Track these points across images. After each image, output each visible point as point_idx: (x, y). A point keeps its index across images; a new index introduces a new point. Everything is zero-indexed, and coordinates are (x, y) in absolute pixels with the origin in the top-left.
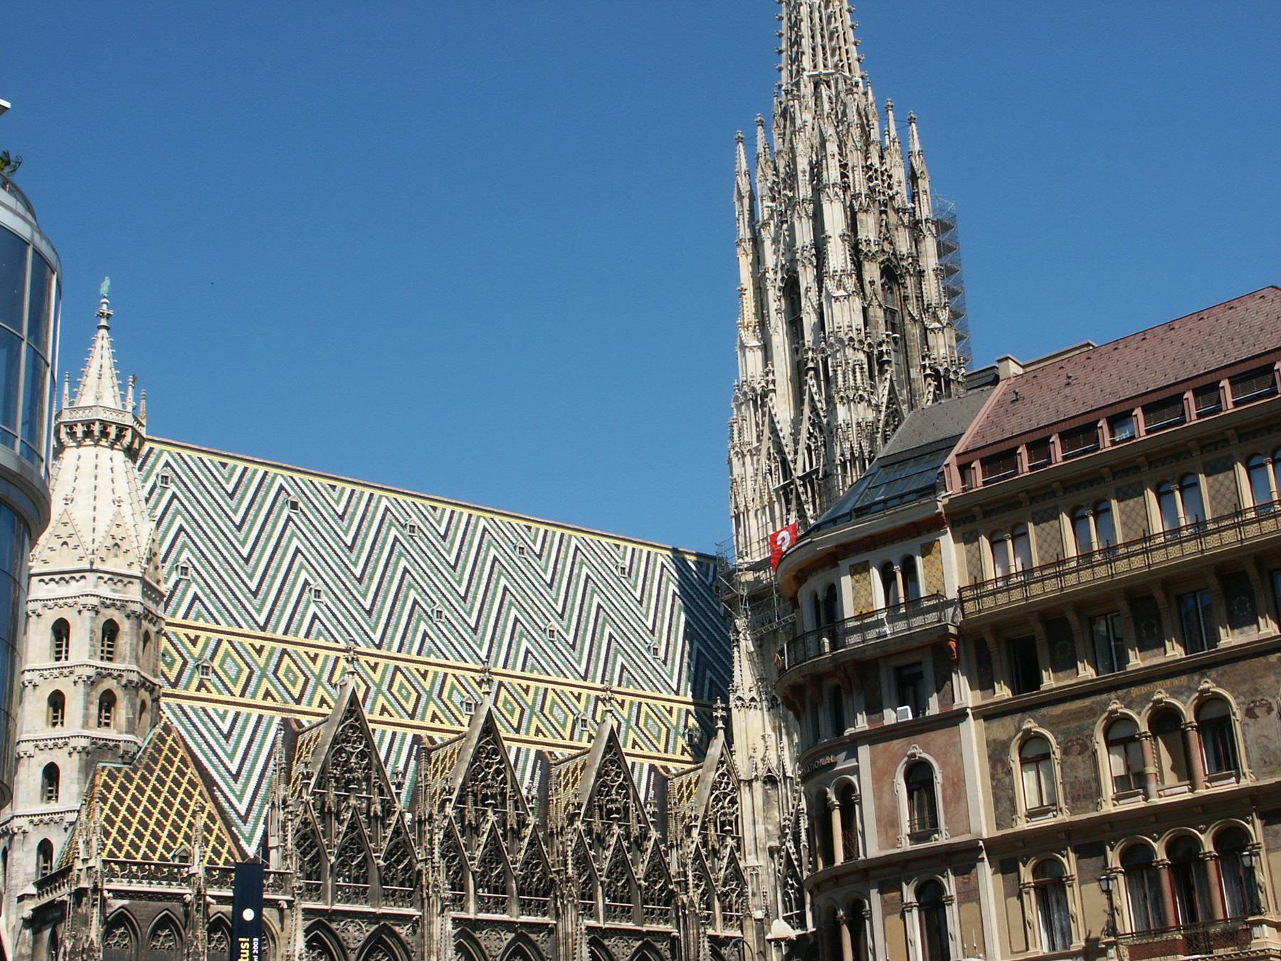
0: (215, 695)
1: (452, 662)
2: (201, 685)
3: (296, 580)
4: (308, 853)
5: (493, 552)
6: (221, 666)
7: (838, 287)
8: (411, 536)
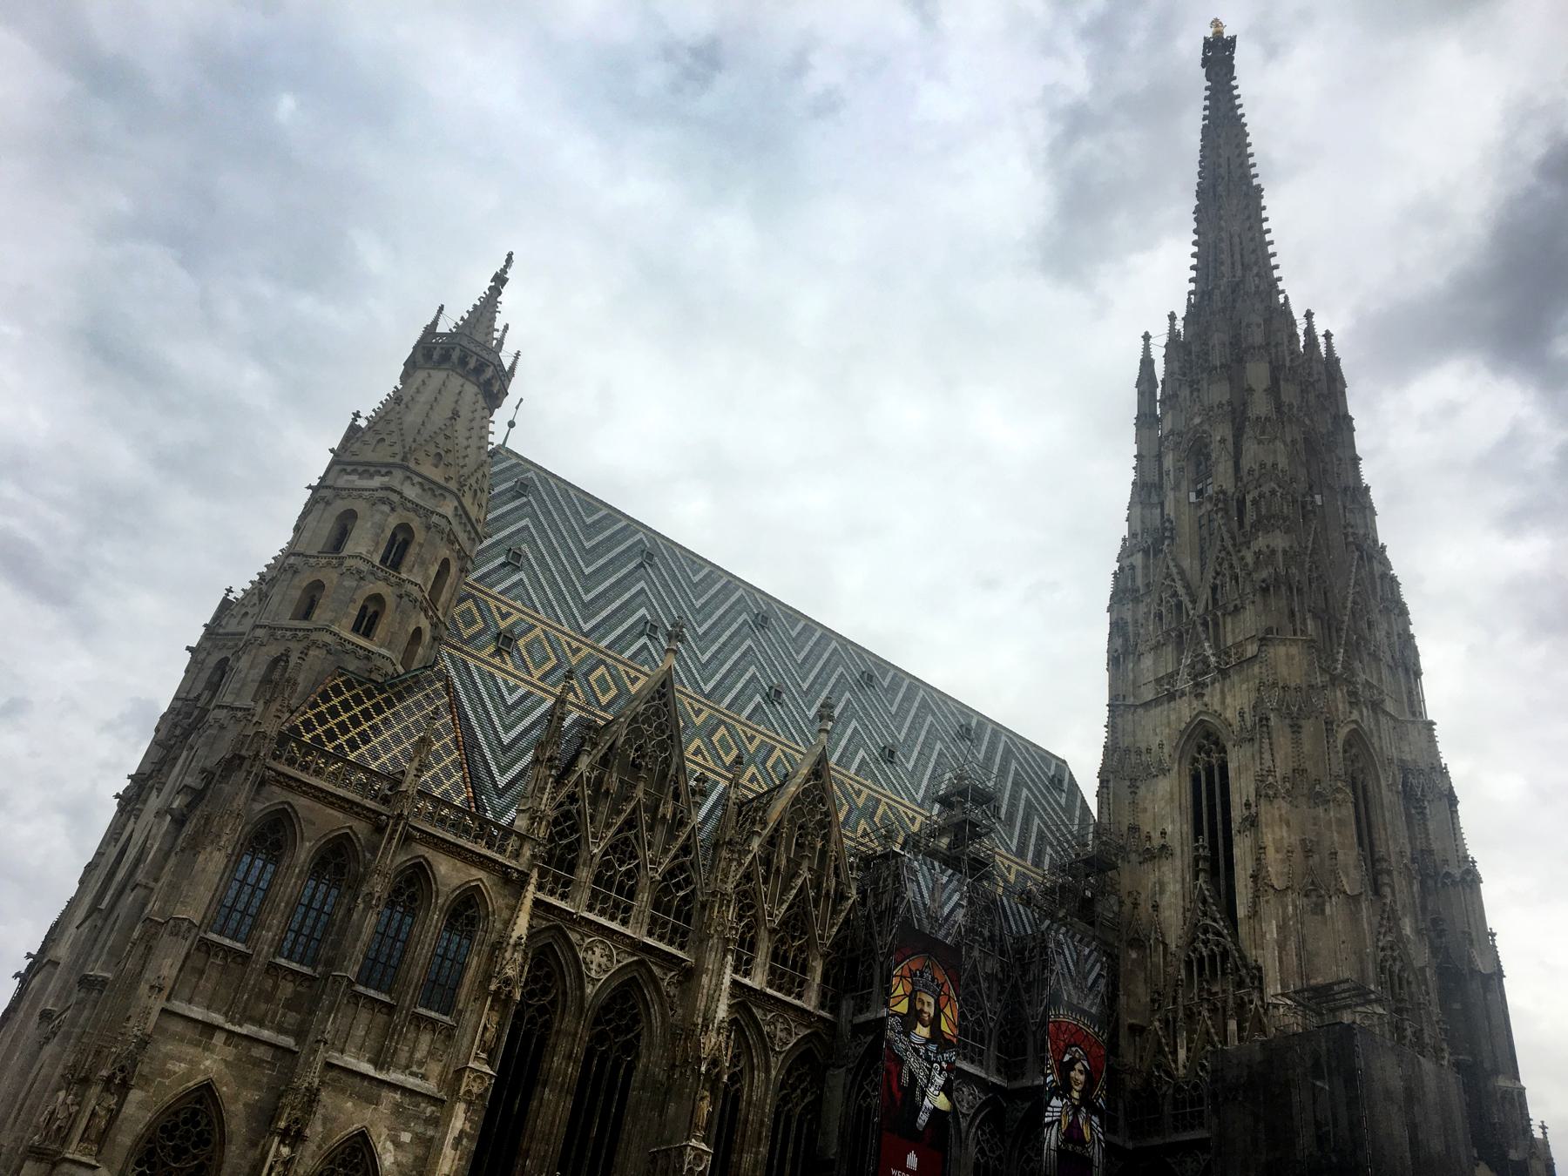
0: (510, 667)
1: (783, 738)
2: (498, 652)
3: (634, 613)
4: (566, 837)
5: (840, 669)
6: (526, 646)
7: (1263, 433)
8: (763, 627)
